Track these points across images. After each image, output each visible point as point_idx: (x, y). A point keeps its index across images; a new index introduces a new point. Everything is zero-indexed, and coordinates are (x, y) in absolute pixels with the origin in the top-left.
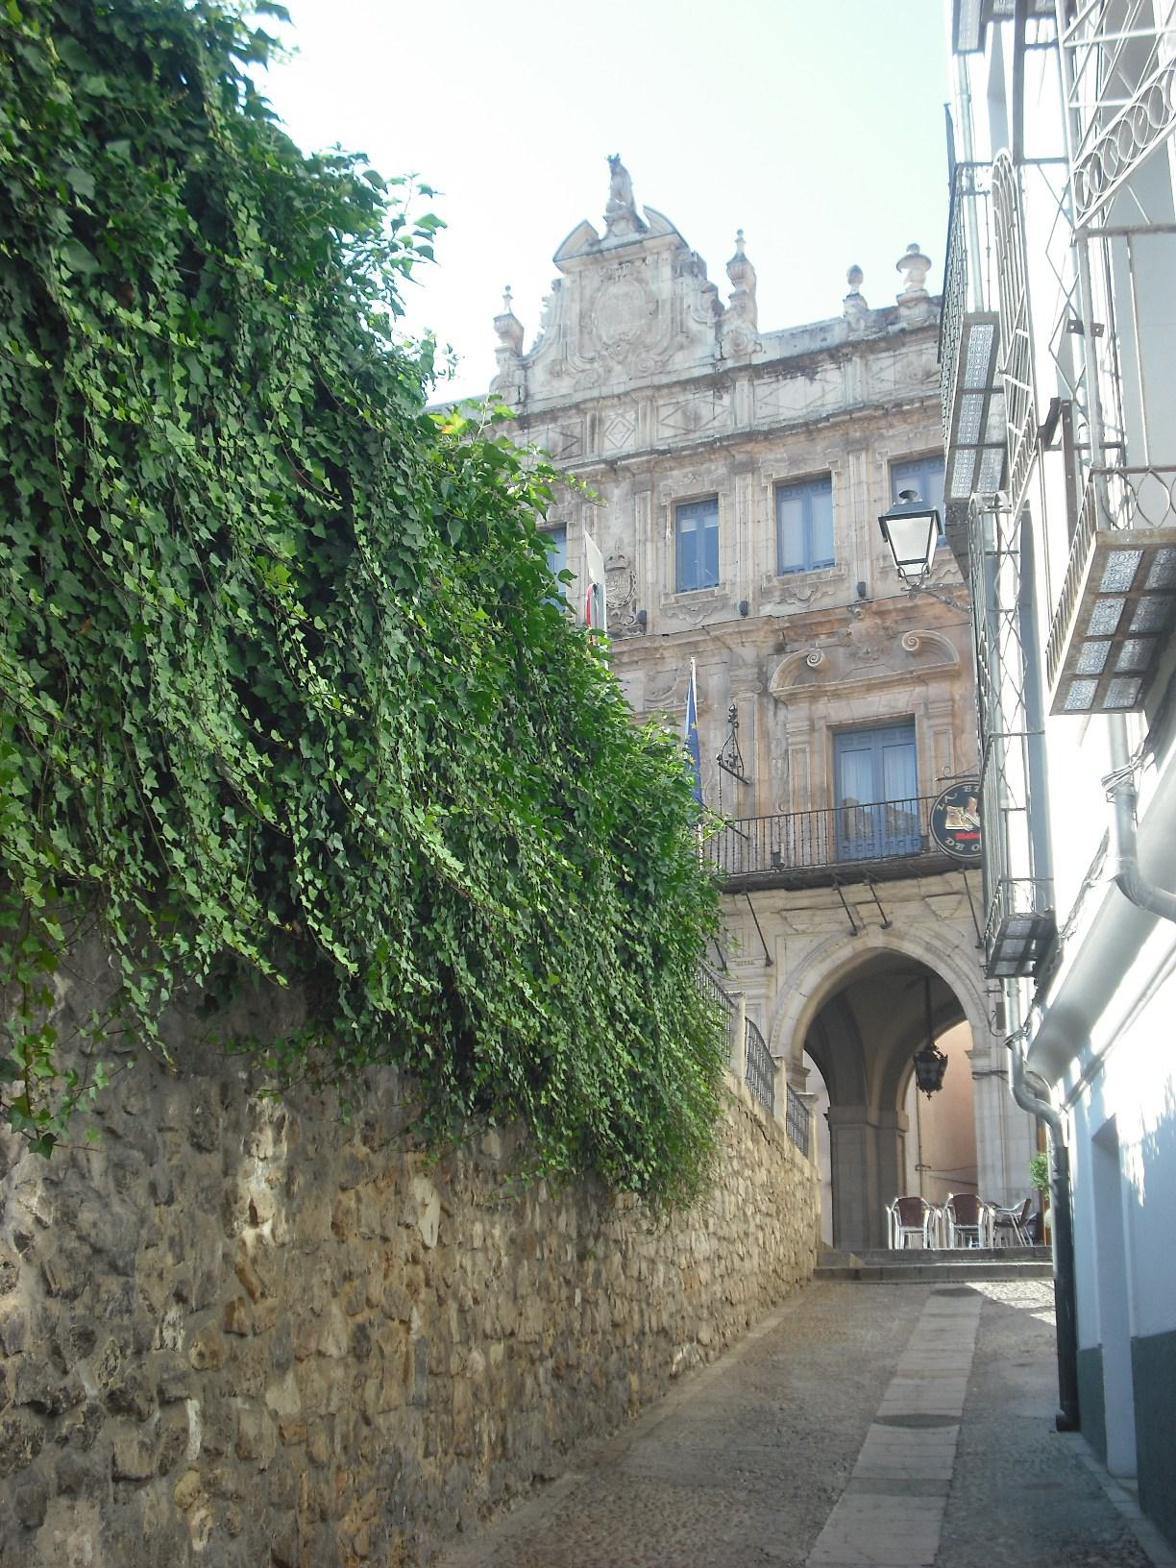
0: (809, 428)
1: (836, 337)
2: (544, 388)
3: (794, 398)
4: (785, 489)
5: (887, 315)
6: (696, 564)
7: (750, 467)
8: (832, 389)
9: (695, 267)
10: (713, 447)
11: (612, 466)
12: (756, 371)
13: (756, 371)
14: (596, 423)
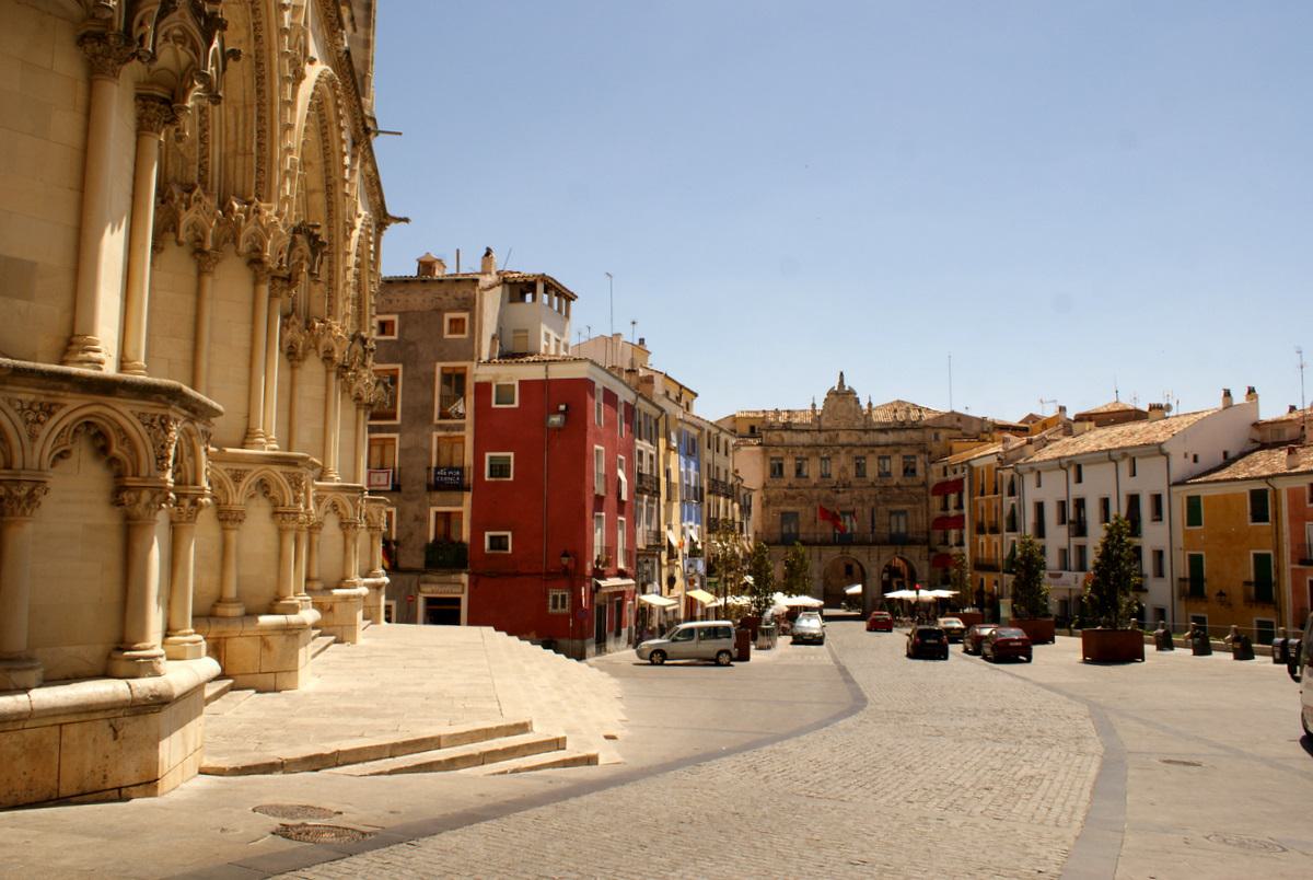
0: (887, 445)
1: (892, 426)
2: (826, 424)
3: (882, 438)
4: (879, 458)
5: (903, 423)
6: (860, 471)
7: (873, 452)
8: (891, 437)
9: (857, 401)
10: (866, 446)
11: (843, 446)
12: (874, 430)
13: (874, 430)
14: (837, 435)
